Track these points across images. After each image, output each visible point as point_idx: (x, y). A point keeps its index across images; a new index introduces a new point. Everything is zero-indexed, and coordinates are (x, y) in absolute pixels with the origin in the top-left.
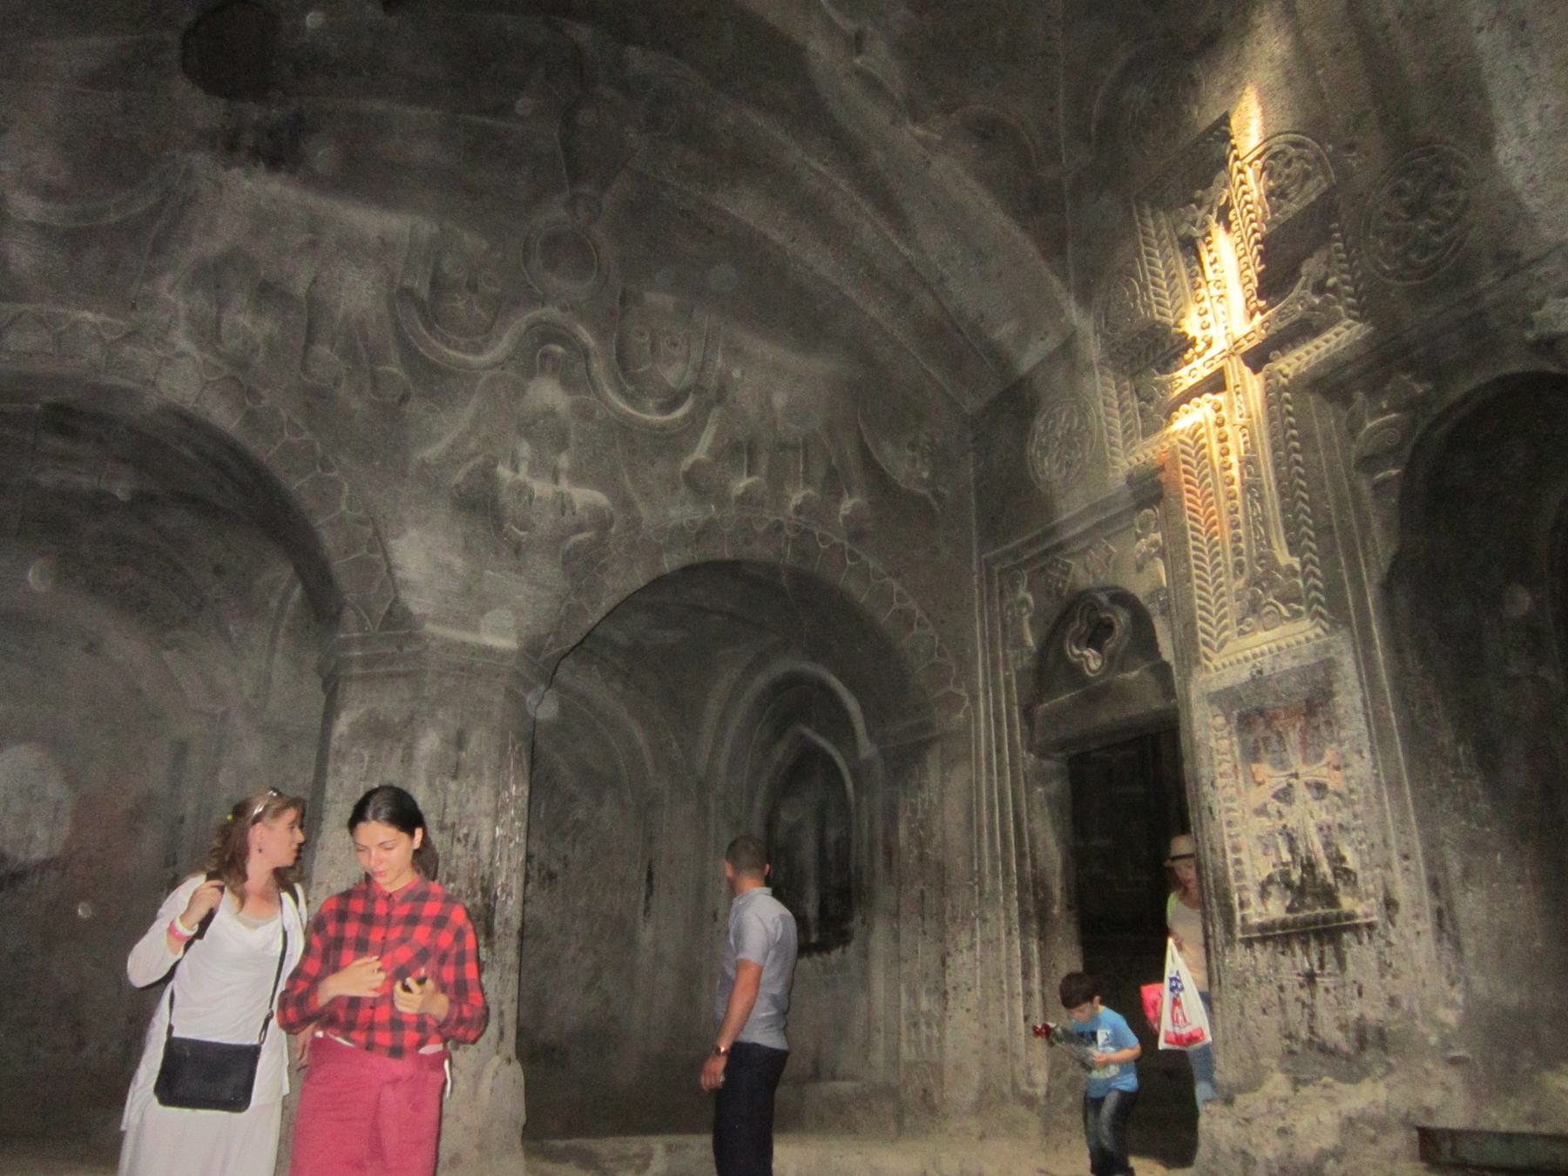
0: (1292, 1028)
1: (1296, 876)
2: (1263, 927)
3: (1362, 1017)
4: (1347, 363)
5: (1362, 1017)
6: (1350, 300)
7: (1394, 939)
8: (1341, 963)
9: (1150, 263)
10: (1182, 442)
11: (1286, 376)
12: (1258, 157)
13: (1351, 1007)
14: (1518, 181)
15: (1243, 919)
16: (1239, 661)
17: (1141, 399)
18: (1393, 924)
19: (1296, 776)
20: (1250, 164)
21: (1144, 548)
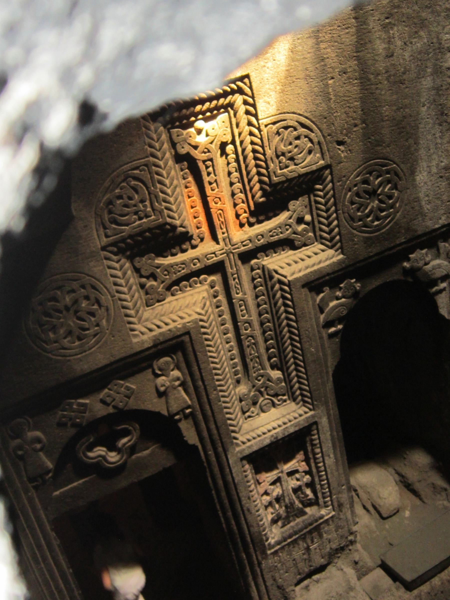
0: (301, 571)
1: (282, 511)
2: (278, 543)
3: (331, 549)
4: (328, 274)
5: (331, 549)
6: (325, 235)
7: (342, 516)
8: (321, 536)
9: (158, 174)
10: (200, 314)
11: (285, 277)
12: (274, 123)
13: (326, 548)
14: (421, 195)
15: (269, 544)
16: (259, 436)
17: (141, 276)
18: (341, 511)
19: (282, 472)
20: (266, 126)
21: (168, 384)
